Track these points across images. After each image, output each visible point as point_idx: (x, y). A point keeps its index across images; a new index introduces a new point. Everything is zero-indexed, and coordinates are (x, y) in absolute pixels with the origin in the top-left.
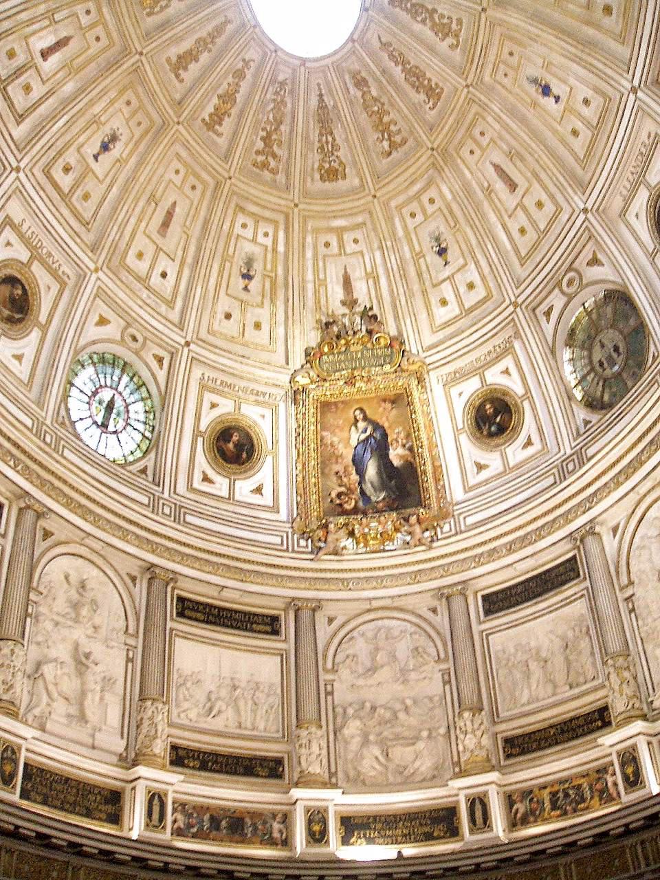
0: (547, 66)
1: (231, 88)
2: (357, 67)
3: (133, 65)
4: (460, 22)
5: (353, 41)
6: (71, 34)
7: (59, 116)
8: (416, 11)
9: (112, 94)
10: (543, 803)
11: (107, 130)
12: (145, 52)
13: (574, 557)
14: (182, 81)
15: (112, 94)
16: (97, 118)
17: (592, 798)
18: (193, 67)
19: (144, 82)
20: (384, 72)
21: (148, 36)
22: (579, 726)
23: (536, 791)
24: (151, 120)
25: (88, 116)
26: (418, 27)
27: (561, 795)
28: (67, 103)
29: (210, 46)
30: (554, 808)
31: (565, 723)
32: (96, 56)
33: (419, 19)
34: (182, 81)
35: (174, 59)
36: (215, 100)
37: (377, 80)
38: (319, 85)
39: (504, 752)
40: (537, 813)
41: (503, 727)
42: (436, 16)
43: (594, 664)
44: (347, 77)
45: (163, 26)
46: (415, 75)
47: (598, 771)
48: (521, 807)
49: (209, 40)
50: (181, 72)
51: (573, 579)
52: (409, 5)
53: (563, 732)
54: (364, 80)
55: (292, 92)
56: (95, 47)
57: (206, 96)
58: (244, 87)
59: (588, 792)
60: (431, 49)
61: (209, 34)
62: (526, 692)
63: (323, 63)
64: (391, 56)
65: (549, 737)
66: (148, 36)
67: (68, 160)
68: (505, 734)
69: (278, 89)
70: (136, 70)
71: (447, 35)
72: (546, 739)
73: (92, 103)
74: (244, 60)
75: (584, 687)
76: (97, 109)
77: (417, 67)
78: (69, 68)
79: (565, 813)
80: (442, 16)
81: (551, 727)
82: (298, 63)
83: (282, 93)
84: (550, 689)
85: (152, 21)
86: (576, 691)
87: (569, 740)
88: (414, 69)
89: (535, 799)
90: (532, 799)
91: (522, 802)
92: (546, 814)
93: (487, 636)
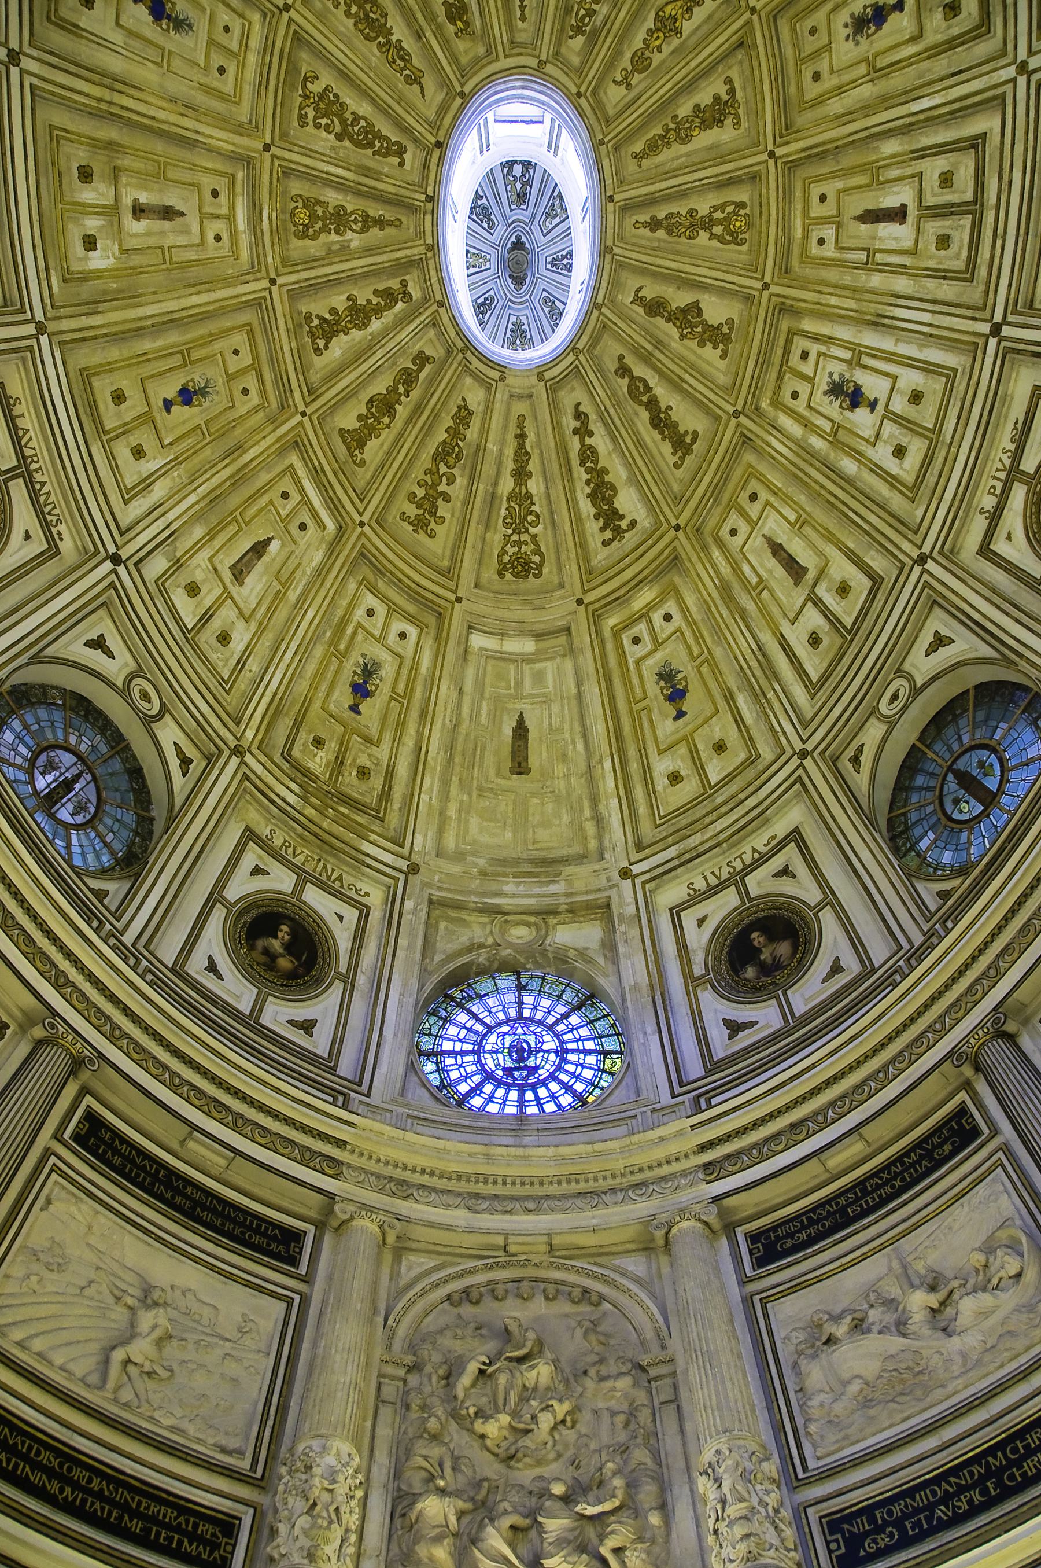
0: (164, 58)
1: (658, 42)
2: (461, 45)
3: (788, 143)
4: (302, 118)
5: (462, 94)
6: (858, 223)
7: (922, 117)
8: (365, 137)
9: (836, 106)
11: (866, 46)
12: (765, 156)
14: (729, 81)
15: (836, 106)
16: (873, 75)
18: (704, 97)
19: (784, 108)
20: (419, 36)
21: (754, 178)
24: (793, 29)
25: (884, 86)
26: (365, 109)
28: (906, 130)
29: (672, 126)
32: (834, 175)
33: (363, 123)
34: (729, 81)
35: (728, 122)
36: (687, 27)
37: (432, 18)
38: (523, 19)
42: (338, 129)
44: (478, 25)
45: (731, 182)
46: (371, 23)
49: (672, 135)
50: (725, 97)
52: (377, 145)
54: (452, 19)
55: (568, 11)
56: (830, 188)
57: (699, 46)
58: (638, 43)
60: (345, 76)
61: (668, 145)
63: (512, 62)
64: (405, 58)
66: (754, 178)
67: (944, 24)
69: (587, 20)
70: (787, 129)
71: (321, 97)
73: (868, 109)
74: (629, 86)
76: (866, 91)
77: (367, 38)
78: (878, 183)
80: (327, 129)
82: (549, 69)
83: (582, 12)
85: (742, 194)
88: (373, 35)
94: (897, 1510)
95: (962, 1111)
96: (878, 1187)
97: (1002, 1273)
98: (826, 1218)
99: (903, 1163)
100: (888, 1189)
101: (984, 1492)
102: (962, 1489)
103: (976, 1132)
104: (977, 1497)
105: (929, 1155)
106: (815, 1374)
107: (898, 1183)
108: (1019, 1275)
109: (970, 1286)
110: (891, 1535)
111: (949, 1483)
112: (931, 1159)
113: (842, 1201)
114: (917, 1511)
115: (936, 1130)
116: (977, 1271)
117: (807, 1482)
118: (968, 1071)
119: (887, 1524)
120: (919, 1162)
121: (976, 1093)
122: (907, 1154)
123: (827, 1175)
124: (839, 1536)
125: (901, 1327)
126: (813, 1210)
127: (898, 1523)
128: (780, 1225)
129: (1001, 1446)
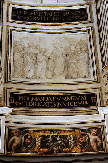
10: (35, 141)
13: (85, 10)
17: (75, 146)
22: (70, 101)
23: (31, 132)
27: (50, 139)
30: (43, 146)
31: (59, 96)
39: (10, 101)
40: (29, 146)
41: (12, 86)
43: (88, 69)
47: (82, 130)
48: (17, 140)
51: (81, 20)
53: (56, 101)
59: (73, 142)
62: (32, 71)
65: (46, 102)
68: (13, 91)
72: (43, 102)
75: (78, 80)
79: (52, 151)
81: (48, 96)
84: (50, 74)
86: (72, 80)
87: (60, 107)
89: (29, 137)
90: (27, 136)
91: (18, 136)
92: (36, 149)
93: (12, 30)
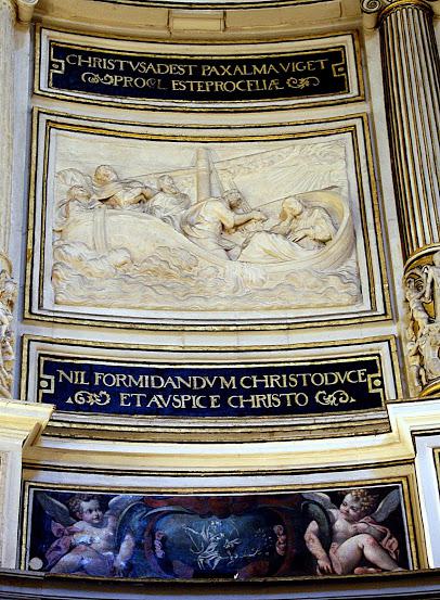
94: (116, 380)
95: (336, 56)
96: (214, 77)
97: (311, 232)
98: (146, 76)
99: (250, 69)
100: (223, 86)
101: (205, 402)
102: (184, 390)
103: (339, 85)
104: (196, 402)
105: (282, 78)
106: (84, 224)
107: (236, 86)
108: (324, 242)
109: (268, 225)
110: (103, 399)
111: (176, 381)
112: (282, 83)
113: (170, 69)
114: (135, 389)
115: (302, 58)
116: (283, 216)
117: (41, 319)
118: (368, 21)
119: (102, 387)
120: (272, 75)
121: (362, 46)
122: (259, 63)
123: (165, 33)
124: (52, 378)
125: (186, 226)
126: (135, 60)
127: (115, 392)
128: (93, 54)
129: (238, 373)
